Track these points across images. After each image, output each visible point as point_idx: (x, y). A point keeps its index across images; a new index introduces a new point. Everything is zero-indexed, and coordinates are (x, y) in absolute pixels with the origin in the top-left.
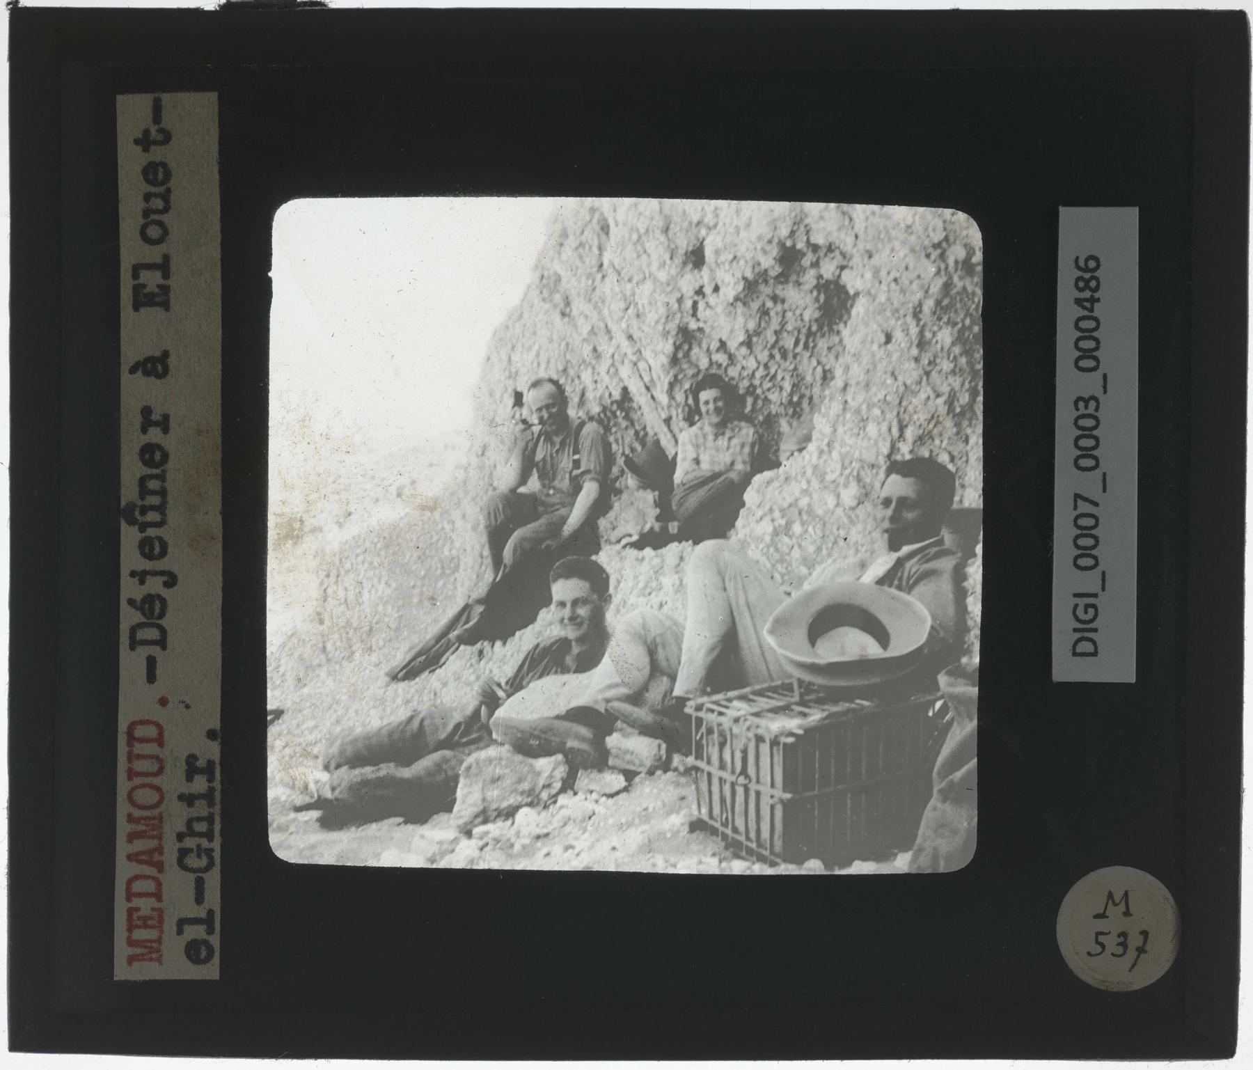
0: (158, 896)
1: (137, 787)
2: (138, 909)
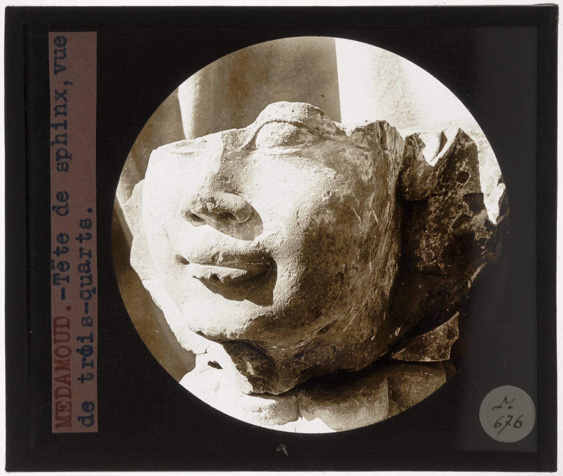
0: (69, 396)
1: (60, 347)
2: (60, 402)
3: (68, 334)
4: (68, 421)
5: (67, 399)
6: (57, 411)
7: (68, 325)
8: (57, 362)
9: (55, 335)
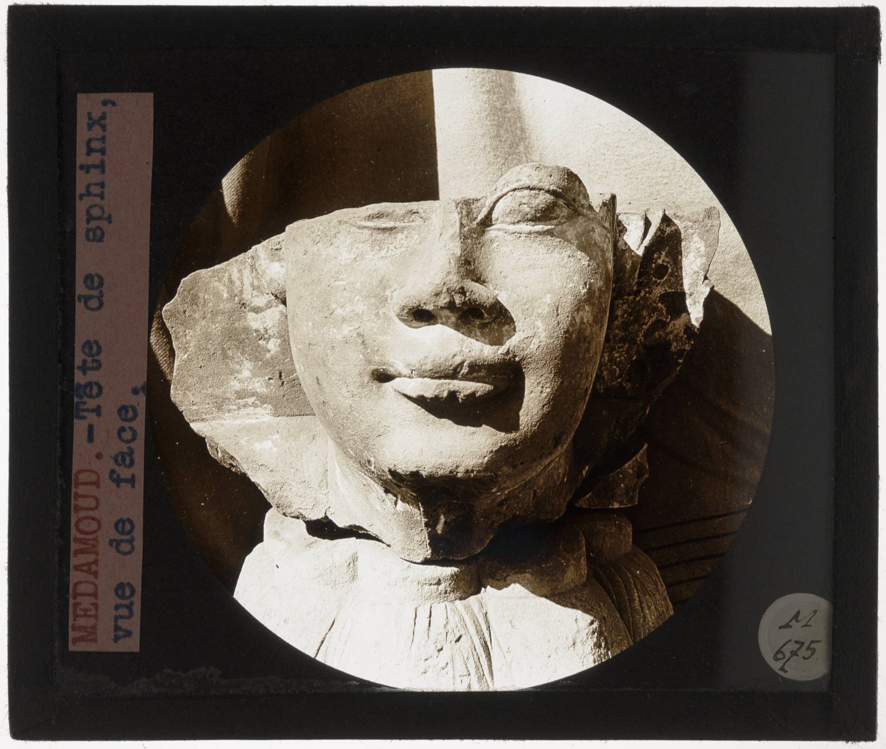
0: (95, 595)
2: (80, 604)
3: (97, 500)
4: (91, 634)
5: (93, 600)
6: (76, 616)
7: (97, 484)
8: (77, 540)
9: (76, 499)
